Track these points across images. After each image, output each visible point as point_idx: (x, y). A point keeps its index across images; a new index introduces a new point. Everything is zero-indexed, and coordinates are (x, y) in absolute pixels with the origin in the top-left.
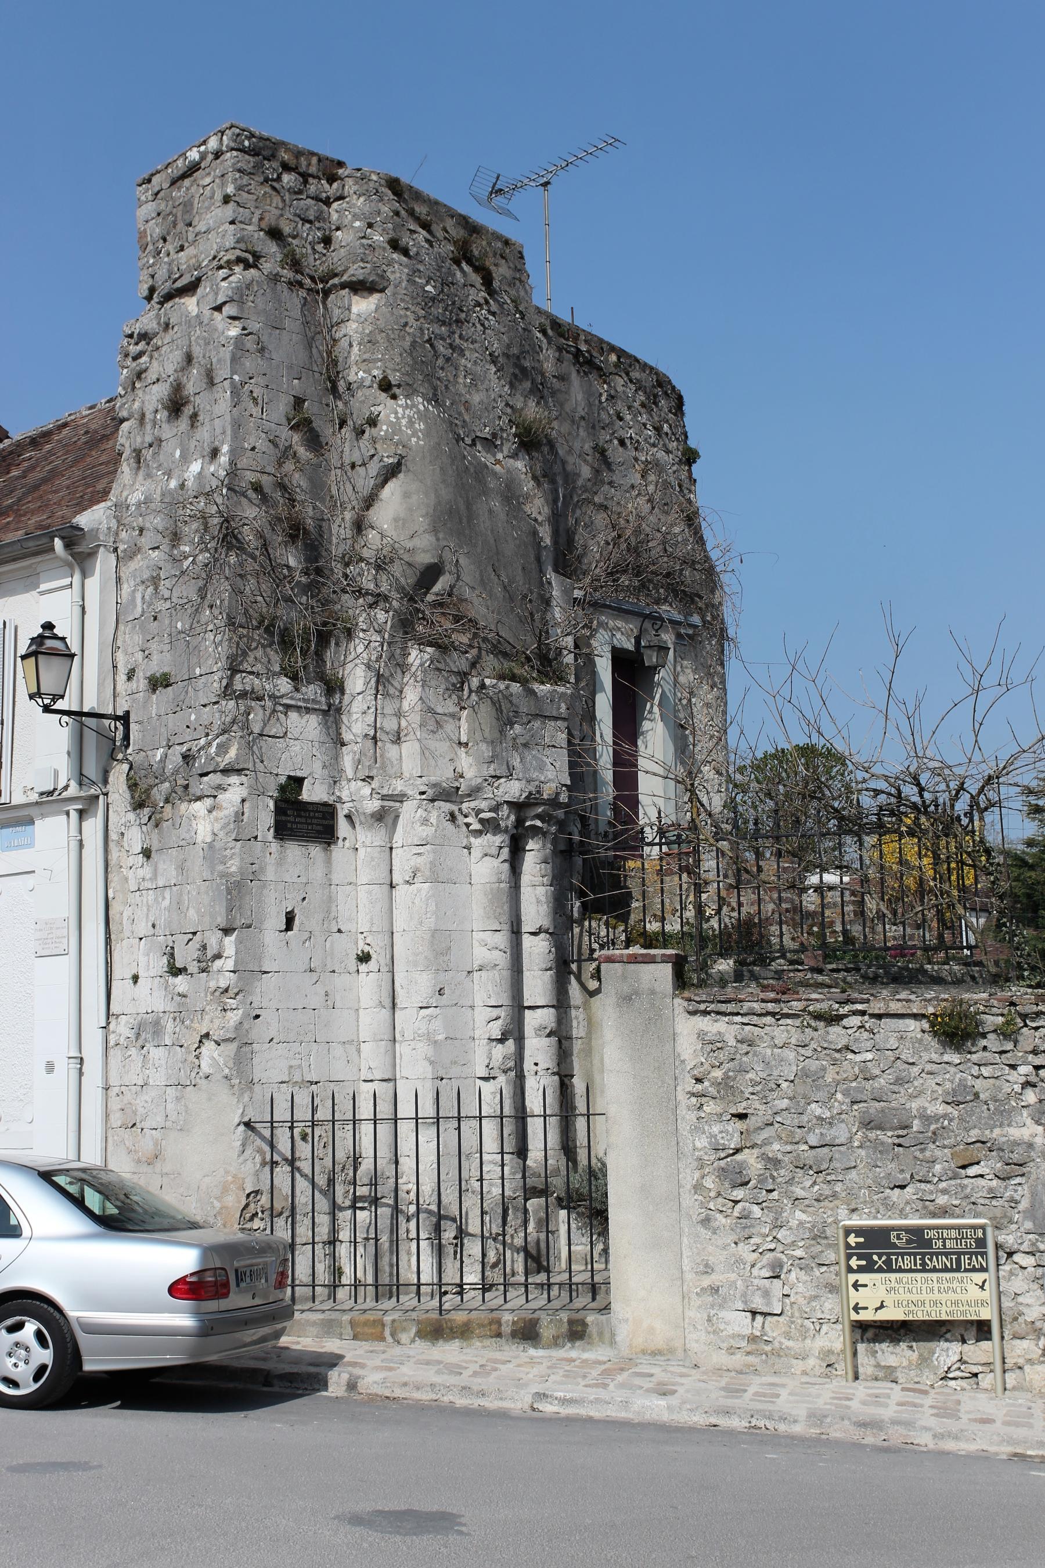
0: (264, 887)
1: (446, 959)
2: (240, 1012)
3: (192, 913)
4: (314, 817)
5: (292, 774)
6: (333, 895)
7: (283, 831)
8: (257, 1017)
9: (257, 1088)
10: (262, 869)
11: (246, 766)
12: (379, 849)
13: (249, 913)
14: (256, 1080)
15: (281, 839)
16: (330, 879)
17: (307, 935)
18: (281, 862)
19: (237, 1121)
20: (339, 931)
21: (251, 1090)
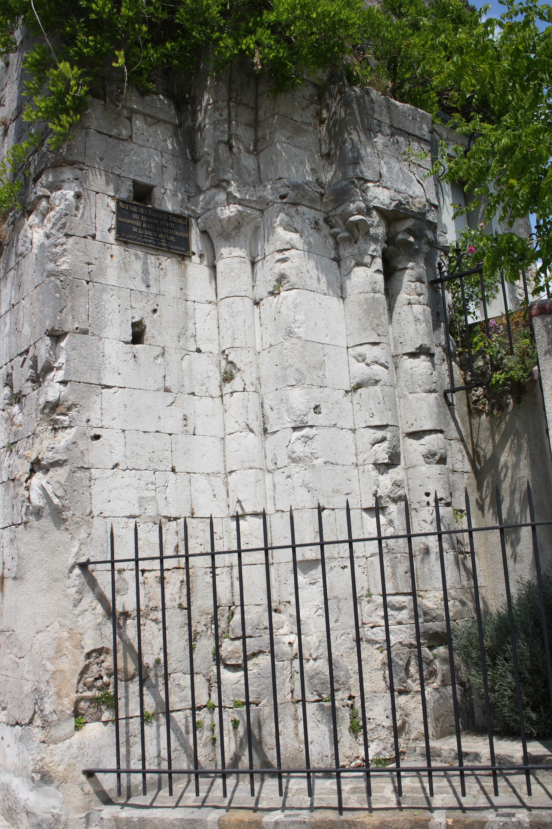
0: (104, 290)
1: (321, 374)
2: (74, 429)
3: (26, 330)
6: (191, 311)
8: (97, 437)
9: (97, 522)
10: (102, 271)
12: (238, 259)
13: (85, 317)
14: (95, 513)
15: (126, 243)
16: (185, 294)
17: (158, 351)
18: (124, 267)
19: (71, 561)
20: (199, 351)
21: (89, 525)
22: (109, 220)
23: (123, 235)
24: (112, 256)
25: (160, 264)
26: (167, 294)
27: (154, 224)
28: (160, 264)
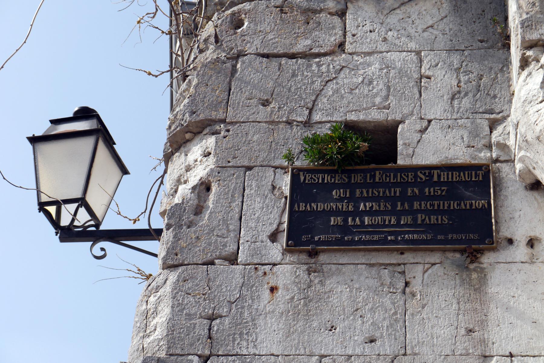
4: (422, 197)
5: (352, 117)
7: (309, 231)
11: (214, 115)
16: (483, 342)
18: (306, 305)
22: (274, 216)
23: (304, 238)
24: (273, 290)
25: (407, 284)
26: (425, 349)
27: (386, 199)
28: (407, 284)
